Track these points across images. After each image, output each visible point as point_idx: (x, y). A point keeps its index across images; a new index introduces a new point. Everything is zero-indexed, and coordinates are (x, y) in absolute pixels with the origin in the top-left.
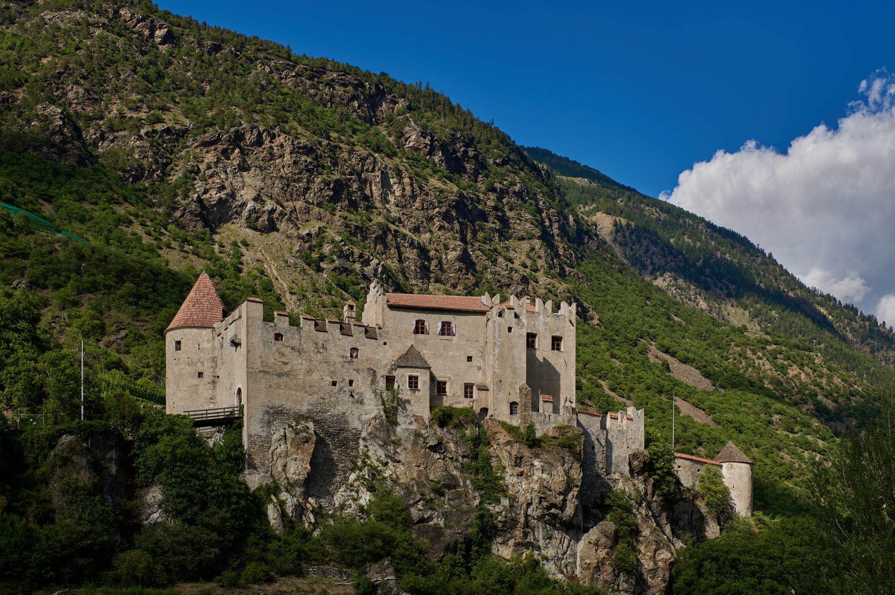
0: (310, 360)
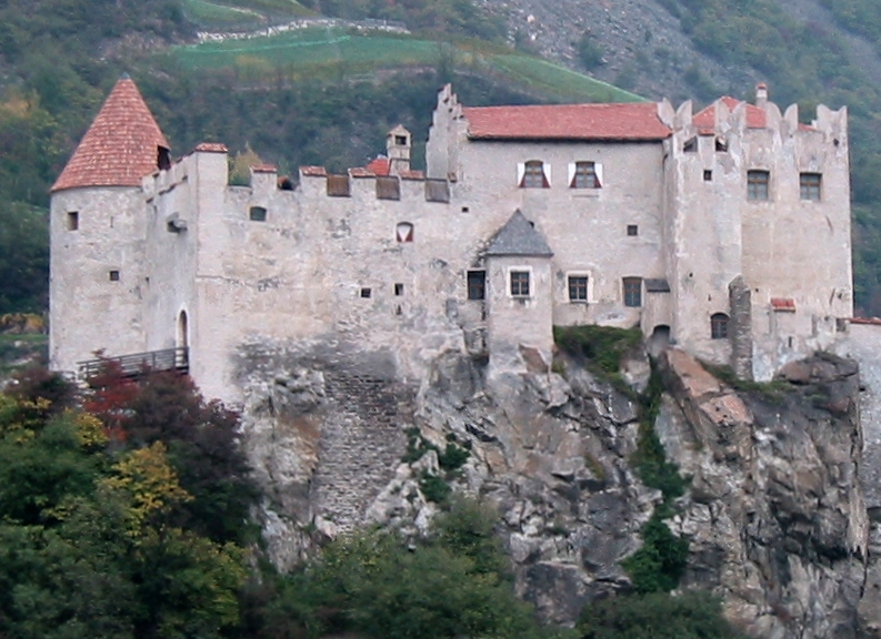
0: (320, 253)
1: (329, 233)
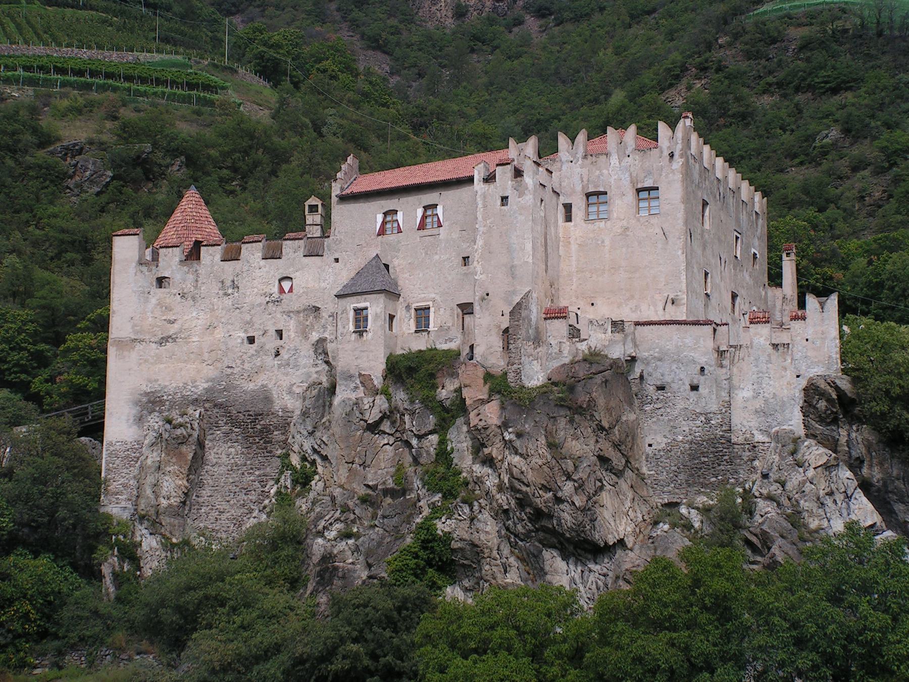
0: (213, 310)
1: (221, 292)
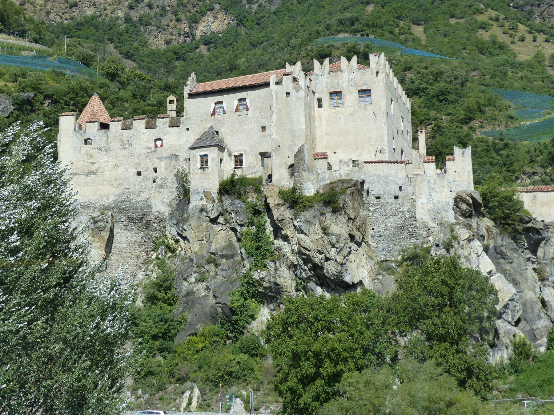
0: (117, 157)
1: (122, 147)
